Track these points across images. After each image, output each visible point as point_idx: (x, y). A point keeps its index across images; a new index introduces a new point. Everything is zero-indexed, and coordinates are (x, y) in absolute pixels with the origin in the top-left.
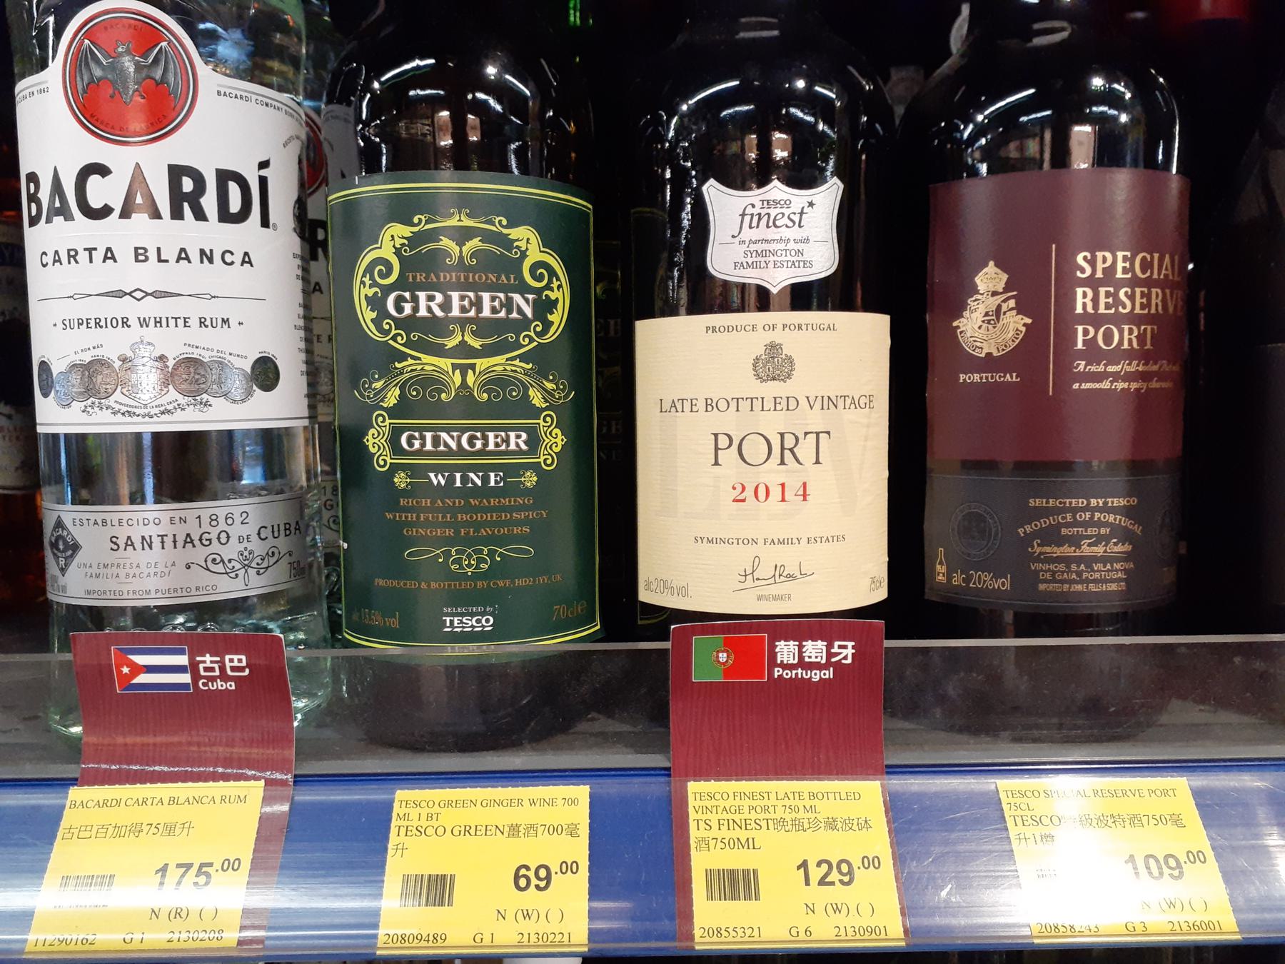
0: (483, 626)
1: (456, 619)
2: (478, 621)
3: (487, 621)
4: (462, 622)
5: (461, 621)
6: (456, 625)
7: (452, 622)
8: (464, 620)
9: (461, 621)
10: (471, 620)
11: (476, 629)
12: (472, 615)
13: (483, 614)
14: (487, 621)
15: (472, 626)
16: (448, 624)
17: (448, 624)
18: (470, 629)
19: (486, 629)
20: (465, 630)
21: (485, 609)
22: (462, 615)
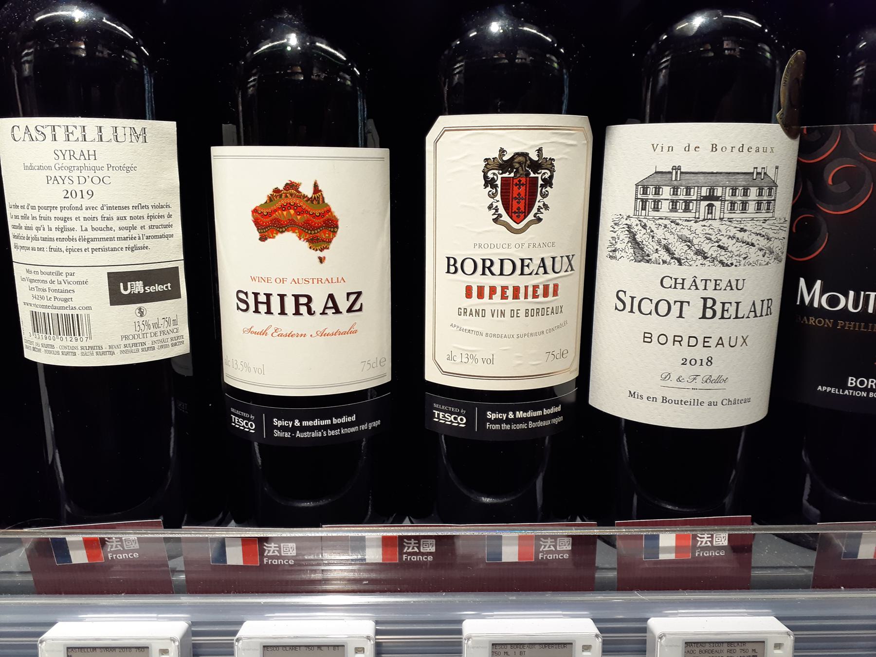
0: (458, 423)
1: (441, 413)
2: (455, 419)
3: (461, 419)
4: (444, 417)
5: (444, 415)
6: (441, 418)
7: (438, 415)
8: (446, 415)
9: (444, 415)
10: (450, 417)
11: (454, 424)
12: (452, 413)
13: (459, 414)
14: (461, 419)
15: (451, 421)
16: (436, 416)
17: (436, 416)
18: (450, 423)
19: (461, 425)
20: (447, 423)
21: (460, 411)
22: (445, 412)
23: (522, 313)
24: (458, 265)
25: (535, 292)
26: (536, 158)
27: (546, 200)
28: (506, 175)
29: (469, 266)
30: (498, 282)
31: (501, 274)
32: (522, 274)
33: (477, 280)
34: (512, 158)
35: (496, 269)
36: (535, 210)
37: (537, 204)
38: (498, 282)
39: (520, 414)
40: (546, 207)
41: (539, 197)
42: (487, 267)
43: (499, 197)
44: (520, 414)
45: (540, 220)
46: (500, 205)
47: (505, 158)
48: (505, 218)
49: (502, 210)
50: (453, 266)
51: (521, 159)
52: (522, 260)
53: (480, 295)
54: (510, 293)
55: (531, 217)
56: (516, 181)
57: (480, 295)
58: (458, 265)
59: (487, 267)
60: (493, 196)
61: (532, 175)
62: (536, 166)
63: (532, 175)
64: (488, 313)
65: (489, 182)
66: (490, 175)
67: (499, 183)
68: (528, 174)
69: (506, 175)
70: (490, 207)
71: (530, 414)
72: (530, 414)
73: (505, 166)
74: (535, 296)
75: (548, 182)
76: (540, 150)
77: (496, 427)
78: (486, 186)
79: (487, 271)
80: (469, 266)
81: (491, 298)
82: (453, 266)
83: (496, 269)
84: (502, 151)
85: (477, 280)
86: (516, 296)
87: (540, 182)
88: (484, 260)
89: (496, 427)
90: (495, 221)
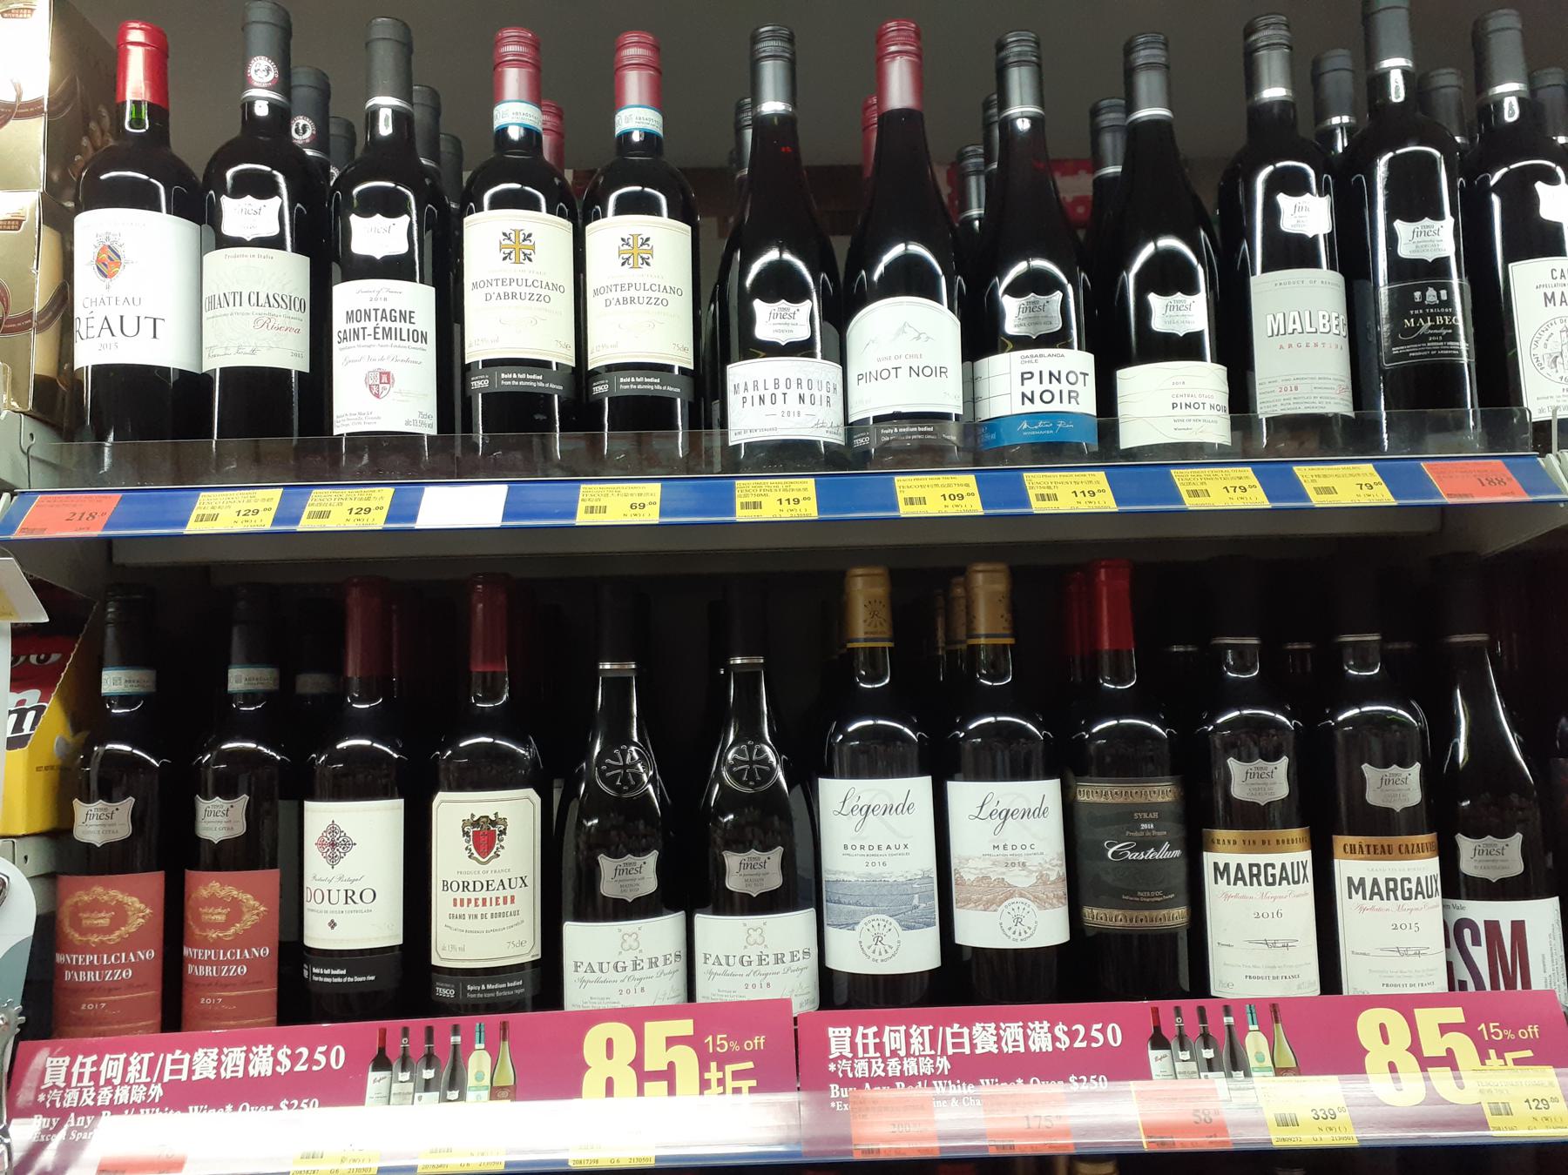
23: (489, 916)
24: (449, 885)
25: (497, 901)
26: (493, 818)
27: (502, 843)
28: (475, 829)
29: (455, 886)
30: (473, 896)
31: (474, 890)
32: (488, 889)
33: (460, 895)
34: (479, 819)
35: (471, 888)
36: (495, 850)
37: (496, 846)
38: (473, 896)
39: (489, 987)
40: (502, 847)
41: (497, 842)
42: (465, 887)
43: (471, 843)
44: (489, 987)
45: (498, 856)
46: (472, 847)
47: (475, 819)
48: (476, 855)
49: (473, 851)
50: (446, 886)
51: (484, 820)
52: (488, 882)
53: (462, 905)
54: (480, 902)
55: (492, 854)
56: (481, 833)
57: (462, 905)
58: (449, 885)
59: (465, 887)
60: (469, 842)
61: (492, 829)
62: (494, 823)
63: (492, 829)
64: (467, 917)
65: (466, 834)
66: (466, 829)
67: (471, 834)
68: (489, 829)
69: (475, 829)
70: (466, 849)
71: (496, 986)
72: (496, 986)
73: (476, 824)
74: (497, 904)
75: (503, 832)
76: (496, 814)
77: (473, 996)
78: (464, 836)
79: (465, 889)
80: (455, 886)
81: (468, 906)
82: (446, 886)
83: (471, 888)
84: (473, 816)
85: (460, 895)
86: (484, 904)
87: (498, 833)
88: (464, 882)
89: (473, 996)
90: (470, 857)
